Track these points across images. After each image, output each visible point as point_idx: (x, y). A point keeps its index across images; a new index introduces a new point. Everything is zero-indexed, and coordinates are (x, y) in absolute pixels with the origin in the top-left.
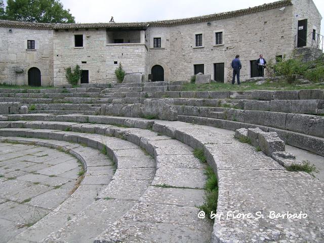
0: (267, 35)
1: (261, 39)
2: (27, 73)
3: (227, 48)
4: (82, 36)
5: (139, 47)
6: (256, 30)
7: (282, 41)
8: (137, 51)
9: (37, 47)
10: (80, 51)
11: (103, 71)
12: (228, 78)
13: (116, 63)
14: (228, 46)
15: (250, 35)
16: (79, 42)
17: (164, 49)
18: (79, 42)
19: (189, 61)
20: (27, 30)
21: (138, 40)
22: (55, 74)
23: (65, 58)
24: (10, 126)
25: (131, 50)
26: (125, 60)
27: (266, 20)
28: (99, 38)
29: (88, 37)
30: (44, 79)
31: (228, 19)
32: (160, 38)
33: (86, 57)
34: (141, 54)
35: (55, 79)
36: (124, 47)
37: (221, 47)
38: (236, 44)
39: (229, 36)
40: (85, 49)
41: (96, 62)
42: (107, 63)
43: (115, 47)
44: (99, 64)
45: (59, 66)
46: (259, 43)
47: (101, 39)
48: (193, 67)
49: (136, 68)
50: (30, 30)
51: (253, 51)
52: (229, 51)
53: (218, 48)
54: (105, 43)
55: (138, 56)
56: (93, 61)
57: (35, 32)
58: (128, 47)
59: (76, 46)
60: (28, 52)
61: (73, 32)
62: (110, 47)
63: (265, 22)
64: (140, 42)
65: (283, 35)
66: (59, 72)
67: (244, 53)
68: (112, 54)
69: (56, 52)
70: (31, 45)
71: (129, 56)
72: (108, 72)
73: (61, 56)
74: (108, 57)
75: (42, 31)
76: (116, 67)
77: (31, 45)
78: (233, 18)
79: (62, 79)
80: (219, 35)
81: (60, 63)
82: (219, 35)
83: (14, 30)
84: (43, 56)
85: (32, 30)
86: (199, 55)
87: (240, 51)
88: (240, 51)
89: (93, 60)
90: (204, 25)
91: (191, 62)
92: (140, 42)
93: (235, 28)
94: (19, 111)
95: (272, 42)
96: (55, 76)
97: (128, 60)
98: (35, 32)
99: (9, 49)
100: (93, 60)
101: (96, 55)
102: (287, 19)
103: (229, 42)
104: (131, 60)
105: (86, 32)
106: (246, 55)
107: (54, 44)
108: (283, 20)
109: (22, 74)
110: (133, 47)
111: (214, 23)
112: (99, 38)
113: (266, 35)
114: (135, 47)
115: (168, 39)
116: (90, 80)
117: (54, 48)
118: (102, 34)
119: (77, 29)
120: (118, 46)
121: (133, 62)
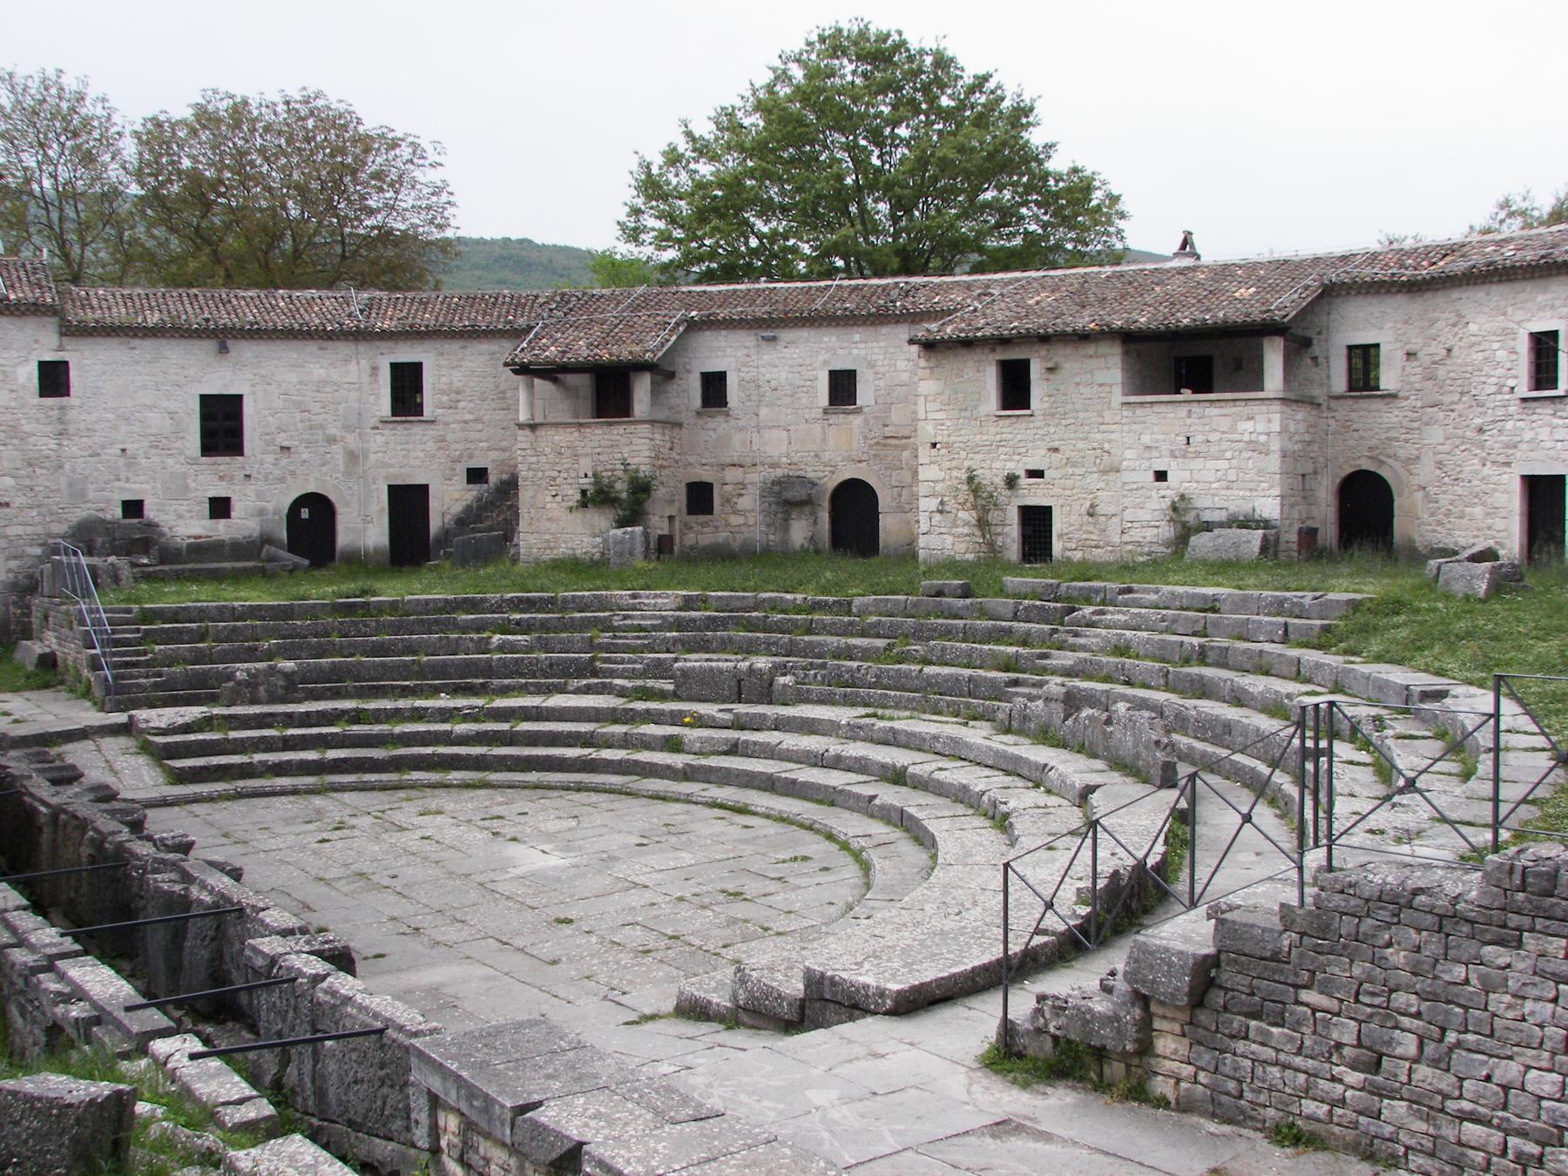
2: (826, 504)
4: (1024, 365)
5: (1255, 408)
8: (1249, 426)
9: (864, 395)
10: (1021, 425)
11: (1112, 510)
13: (1161, 476)
16: (1015, 391)
17: (1394, 396)
18: (1015, 391)
19: (1501, 459)
20: (831, 330)
21: (1254, 380)
22: (923, 518)
23: (963, 454)
24: (734, 749)
25: (1225, 423)
26: (1197, 464)
28: (1091, 372)
29: (1050, 370)
30: (889, 525)
32: (1377, 346)
33: (1043, 452)
34: (1263, 438)
35: (922, 541)
36: (1196, 408)
40: (1038, 421)
41: (1078, 471)
42: (1127, 476)
43: (1157, 408)
44: (1094, 481)
45: (939, 487)
47: (1100, 376)
48: (1516, 486)
49: (1244, 498)
50: (840, 331)
54: (1118, 397)
55: (1255, 447)
56: (1070, 471)
57: (857, 334)
58: (1212, 411)
59: (1004, 408)
60: (833, 419)
61: (993, 350)
62: (1139, 412)
64: (1262, 390)
66: (941, 512)
68: (1146, 439)
69: (928, 431)
70: (843, 387)
71: (1214, 449)
72: (1128, 515)
73: (948, 446)
74: (1130, 454)
75: (885, 330)
76: (1158, 499)
77: (843, 387)
79: (949, 539)
81: (941, 475)
83: (786, 335)
84: (888, 431)
85: (849, 330)
89: (1069, 462)
91: (1508, 464)
92: (1262, 390)
94: (767, 693)
96: (924, 527)
97: (1211, 464)
98: (857, 337)
99: (763, 412)
100: (1069, 462)
101: (1081, 445)
104: (1222, 464)
105: (1044, 350)
107: (921, 400)
109: (807, 509)
110: (1230, 409)
112: (1091, 372)
114: (1239, 409)
115: (1411, 347)
116: (1057, 547)
117: (921, 415)
118: (1104, 356)
119: (1004, 341)
120: (1170, 407)
121: (1232, 475)
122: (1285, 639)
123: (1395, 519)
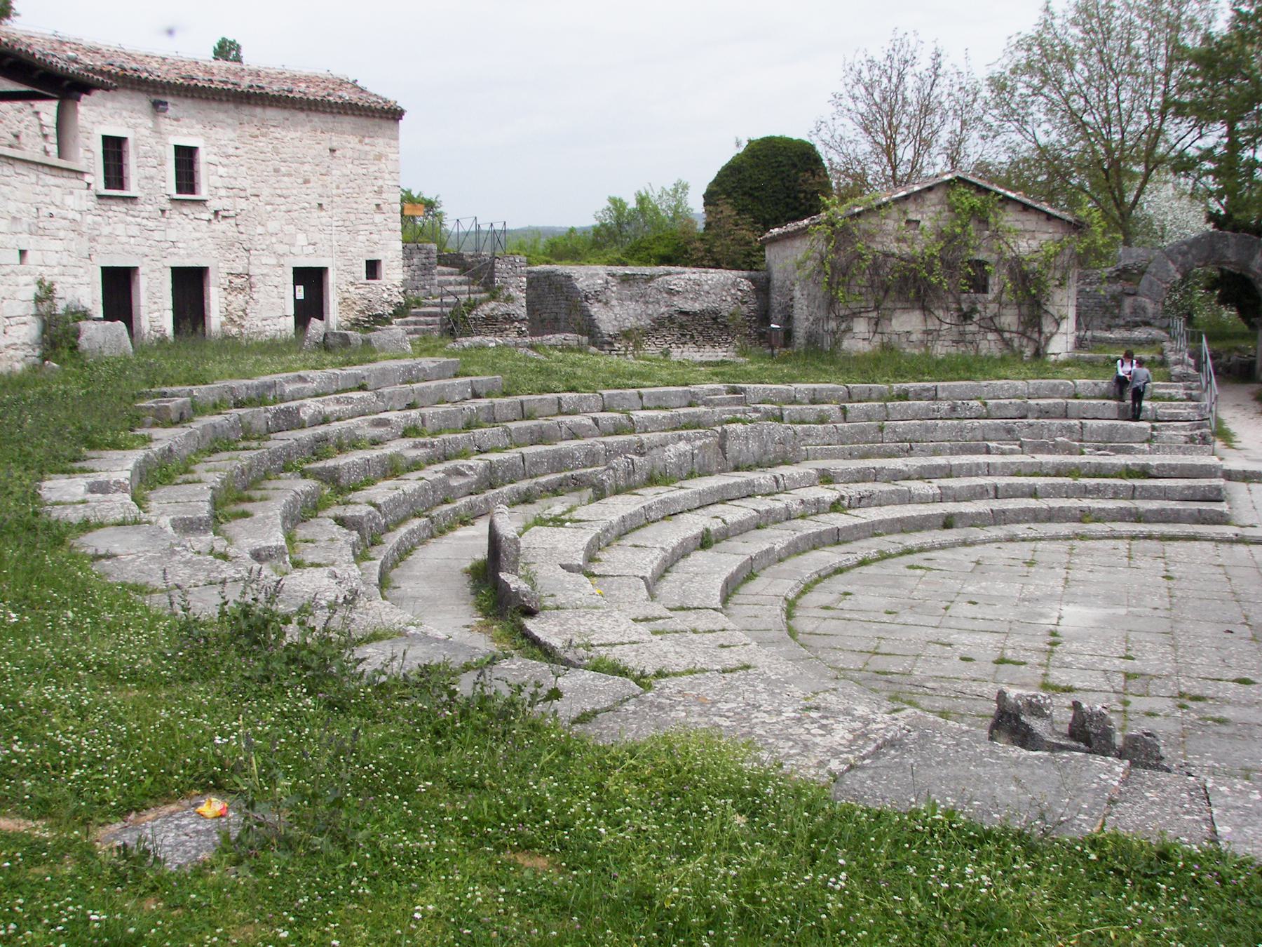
0: (340, 191)
1: (324, 201)
3: (216, 213)
6: (307, 167)
7: (378, 218)
12: (223, 324)
14: (214, 204)
15: (286, 179)
27: (335, 145)
31: (215, 105)
37: (194, 208)
38: (242, 204)
39: (221, 170)
46: (316, 213)
51: (301, 239)
52: (221, 226)
53: (185, 210)
63: (332, 151)
65: (379, 202)
67: (274, 240)
78: (231, 106)
80: (186, 158)
82: (186, 158)
86: (120, 229)
87: (260, 230)
88: (260, 230)
90: (142, 102)
93: (237, 145)
95: (352, 217)
102: (386, 156)
103: (223, 192)
106: (281, 249)
108: (379, 157)
111: (175, 106)
113: (335, 191)
122: (476, 395)
123: (171, 306)
